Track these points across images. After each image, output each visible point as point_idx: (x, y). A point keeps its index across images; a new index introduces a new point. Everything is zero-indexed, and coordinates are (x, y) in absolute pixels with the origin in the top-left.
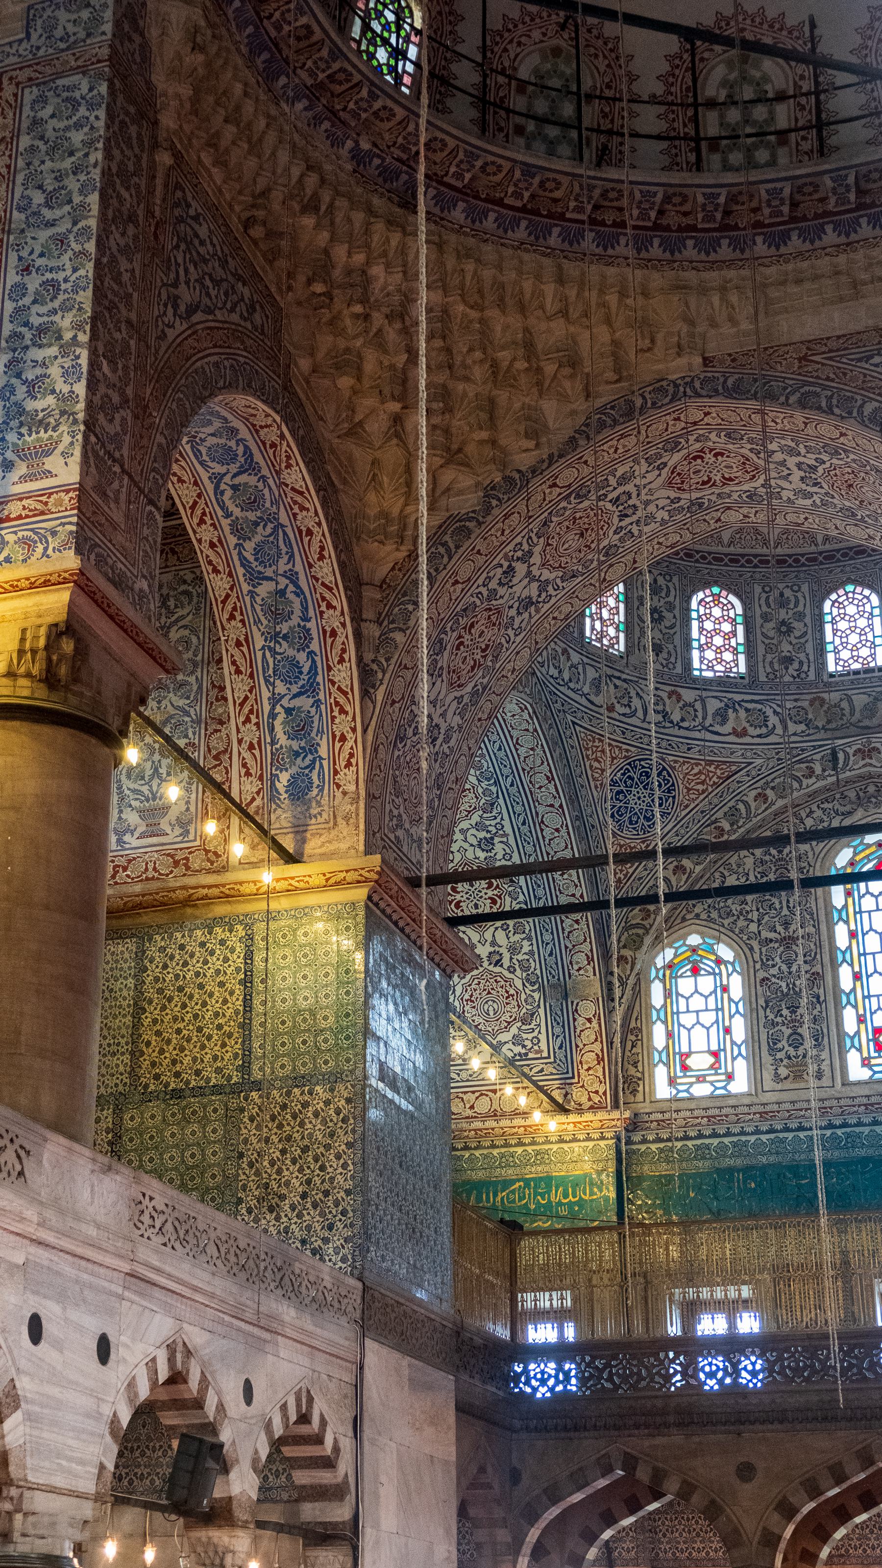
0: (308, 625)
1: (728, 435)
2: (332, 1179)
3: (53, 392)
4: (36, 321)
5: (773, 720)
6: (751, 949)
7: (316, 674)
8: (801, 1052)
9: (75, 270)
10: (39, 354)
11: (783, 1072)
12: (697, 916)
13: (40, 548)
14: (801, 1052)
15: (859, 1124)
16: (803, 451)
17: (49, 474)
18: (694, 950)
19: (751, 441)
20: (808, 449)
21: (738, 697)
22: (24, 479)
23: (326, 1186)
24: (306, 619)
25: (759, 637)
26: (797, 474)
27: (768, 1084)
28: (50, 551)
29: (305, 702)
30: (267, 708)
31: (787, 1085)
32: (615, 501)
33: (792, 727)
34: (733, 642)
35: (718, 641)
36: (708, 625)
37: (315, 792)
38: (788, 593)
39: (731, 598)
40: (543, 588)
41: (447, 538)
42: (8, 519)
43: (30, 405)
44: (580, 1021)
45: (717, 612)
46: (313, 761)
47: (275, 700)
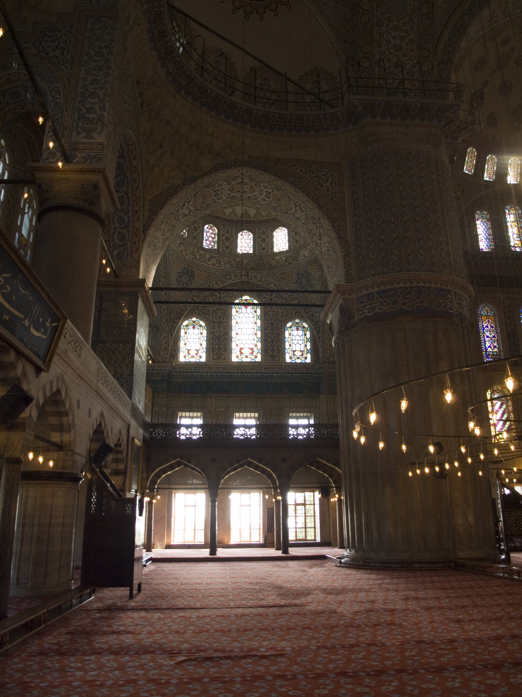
1: (250, 179)
2: (123, 372)
3: (96, 113)
5: (222, 263)
6: (210, 323)
8: (220, 352)
9: (105, 77)
12: (196, 313)
13: (89, 160)
14: (220, 352)
15: (234, 373)
16: (269, 187)
17: (93, 138)
18: (194, 322)
19: (256, 182)
20: (271, 188)
21: (214, 255)
22: (84, 138)
24: (128, 206)
25: (221, 240)
27: (211, 360)
28: (93, 162)
29: (125, 231)
30: (112, 231)
31: (216, 360)
32: (215, 191)
33: (227, 266)
34: (214, 240)
35: (210, 239)
36: (208, 234)
37: (125, 258)
38: (229, 230)
40: (189, 212)
42: (78, 149)
43: (87, 115)
44: (162, 337)
45: (211, 231)
46: (125, 249)
47: (115, 229)
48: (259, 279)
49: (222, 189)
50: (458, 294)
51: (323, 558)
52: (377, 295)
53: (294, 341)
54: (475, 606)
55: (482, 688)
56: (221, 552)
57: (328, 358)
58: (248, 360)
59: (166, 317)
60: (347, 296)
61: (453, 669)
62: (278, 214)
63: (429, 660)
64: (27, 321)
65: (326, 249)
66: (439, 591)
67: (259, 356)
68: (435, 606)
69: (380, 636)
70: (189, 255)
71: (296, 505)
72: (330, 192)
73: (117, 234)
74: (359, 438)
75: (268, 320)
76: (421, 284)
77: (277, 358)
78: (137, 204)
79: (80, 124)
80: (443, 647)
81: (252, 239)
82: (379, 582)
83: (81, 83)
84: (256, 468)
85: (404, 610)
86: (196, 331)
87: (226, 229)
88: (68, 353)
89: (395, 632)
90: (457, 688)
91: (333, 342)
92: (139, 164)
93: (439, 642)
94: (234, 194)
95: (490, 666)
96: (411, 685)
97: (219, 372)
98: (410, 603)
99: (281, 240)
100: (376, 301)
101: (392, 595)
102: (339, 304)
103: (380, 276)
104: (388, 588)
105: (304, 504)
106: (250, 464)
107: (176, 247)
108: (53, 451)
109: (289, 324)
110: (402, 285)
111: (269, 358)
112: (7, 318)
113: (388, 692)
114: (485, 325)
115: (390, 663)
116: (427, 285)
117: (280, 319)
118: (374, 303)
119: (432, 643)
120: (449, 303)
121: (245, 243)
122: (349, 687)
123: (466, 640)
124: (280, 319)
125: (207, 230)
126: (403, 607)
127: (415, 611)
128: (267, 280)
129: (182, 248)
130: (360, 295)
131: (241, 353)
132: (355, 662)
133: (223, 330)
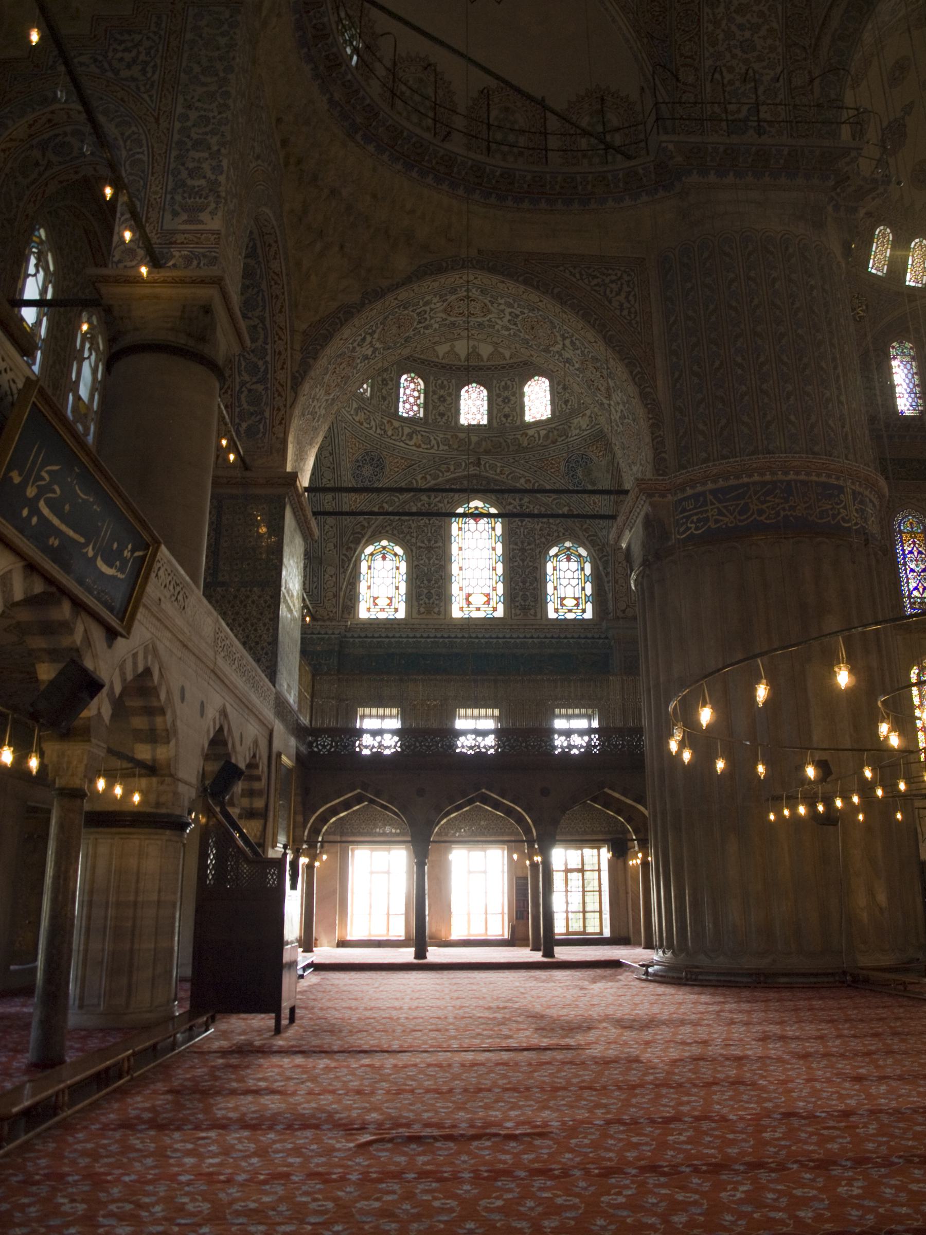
0: (267, 347)
1: (482, 291)
2: (261, 636)
3: (205, 177)
4: (195, 137)
7: (267, 373)
8: (431, 601)
9: (220, 113)
10: (197, 155)
11: (422, 610)
12: (387, 532)
13: (195, 262)
15: (456, 637)
16: (516, 306)
17: (201, 222)
18: (384, 548)
19: (492, 297)
21: (418, 429)
22: (185, 222)
23: (257, 639)
26: (508, 317)
27: (415, 615)
28: (202, 264)
29: (260, 387)
30: (237, 388)
31: (424, 616)
32: (419, 314)
34: (418, 402)
35: (412, 400)
37: (261, 435)
38: (445, 382)
39: (419, 380)
40: (374, 352)
41: (340, 315)
42: (175, 243)
43: (190, 182)
44: (327, 576)
45: (412, 386)
47: (243, 384)
48: (498, 471)
49: (432, 310)
50: (859, 493)
51: (615, 964)
52: (711, 497)
53: (562, 581)
54: (890, 1052)
55: (903, 1197)
56: (435, 954)
57: (624, 611)
58: (481, 614)
59: (334, 540)
60: (657, 499)
61: (849, 1164)
62: (533, 353)
63: (805, 1147)
64: (91, 547)
65: (619, 414)
66: (823, 1026)
67: (501, 607)
68: (817, 1052)
69: (718, 1103)
70: (374, 429)
71: (567, 871)
72: (625, 312)
73: (246, 393)
74: (680, 752)
75: (516, 544)
76: (791, 476)
77: (532, 612)
78: (280, 339)
79: (178, 198)
80: (831, 1123)
81: (486, 398)
82: (717, 1008)
83: (178, 125)
84: (497, 805)
85: (760, 1057)
86: (389, 564)
87: (439, 382)
88: (163, 605)
89: (745, 1097)
90: (858, 1197)
91: (632, 582)
92: (284, 268)
93: (823, 1115)
94: (453, 319)
95: (916, 1160)
96: (774, 1191)
97: (428, 637)
98: (770, 1046)
99: (537, 400)
100: (710, 507)
101: (738, 1032)
102: (643, 514)
103: (717, 463)
104: (732, 1019)
105: (582, 871)
106: (485, 800)
107: (351, 415)
108: (140, 776)
109: (554, 551)
110: (756, 478)
111: (518, 612)
112: (57, 543)
113: (734, 1202)
114: (907, 549)
115: (736, 1151)
116: (802, 477)
117: (538, 542)
118: (707, 511)
119: (811, 1117)
120: (841, 510)
121: (473, 406)
122: (663, 1191)
123: (872, 1112)
124: (538, 542)
125: (406, 384)
126: (760, 1052)
127: (779, 1060)
128: (514, 472)
129: (361, 417)
130: (680, 496)
131: (469, 603)
132: (674, 1149)
133: (436, 562)
